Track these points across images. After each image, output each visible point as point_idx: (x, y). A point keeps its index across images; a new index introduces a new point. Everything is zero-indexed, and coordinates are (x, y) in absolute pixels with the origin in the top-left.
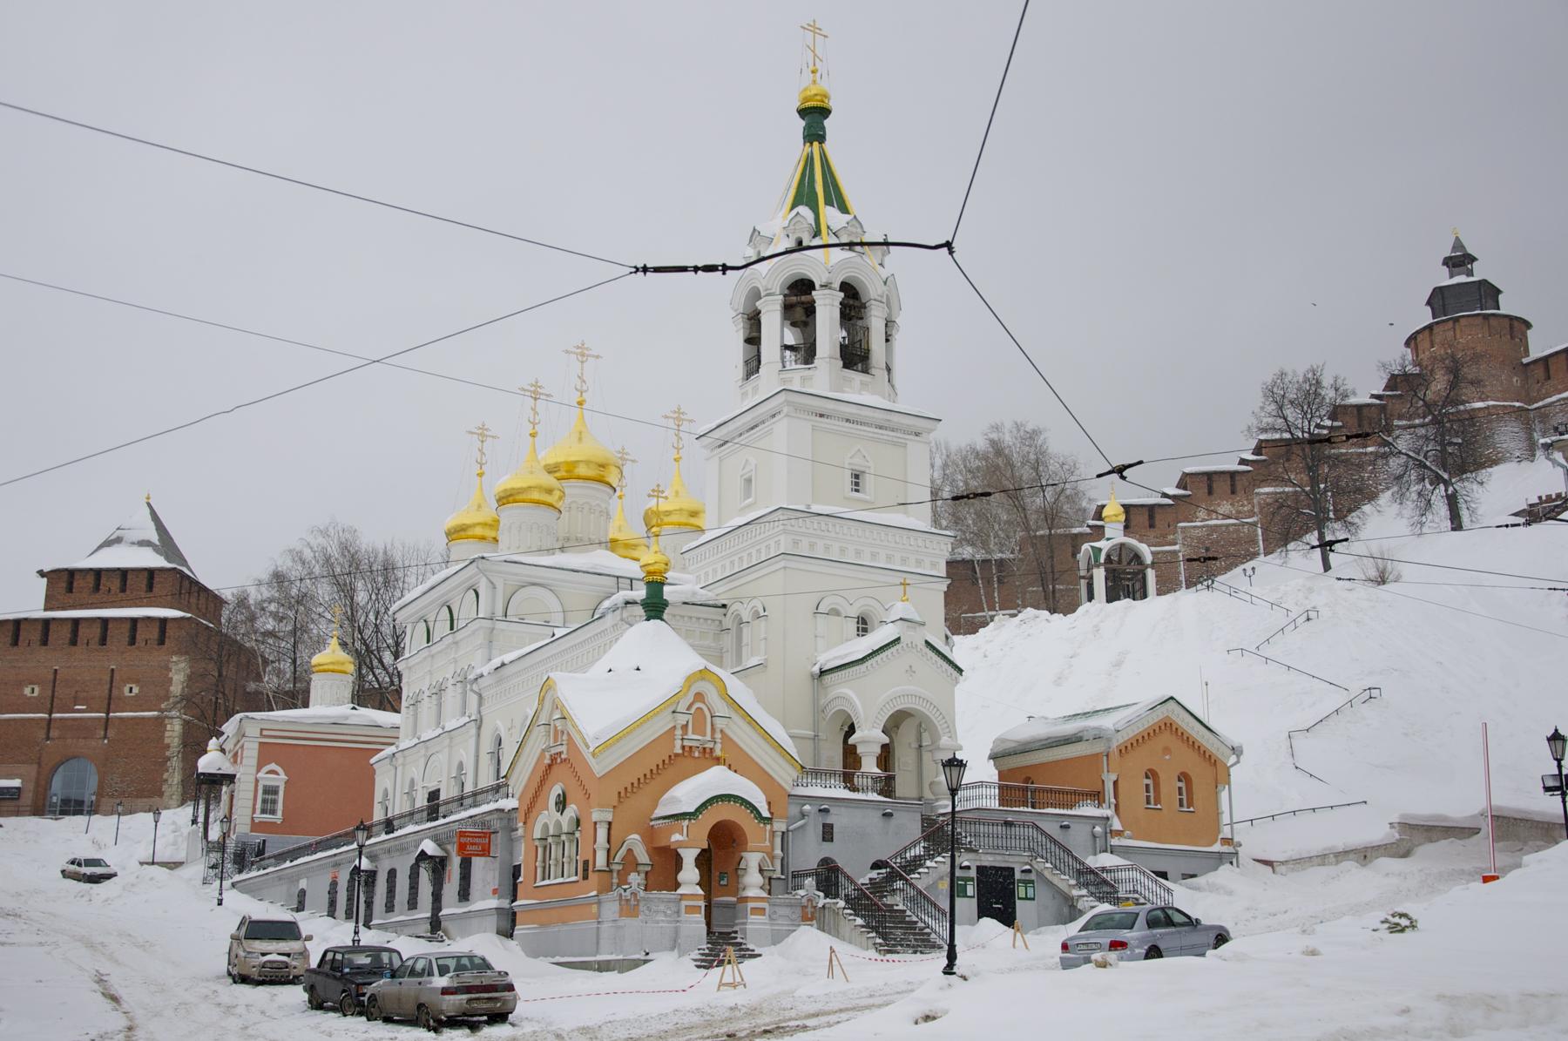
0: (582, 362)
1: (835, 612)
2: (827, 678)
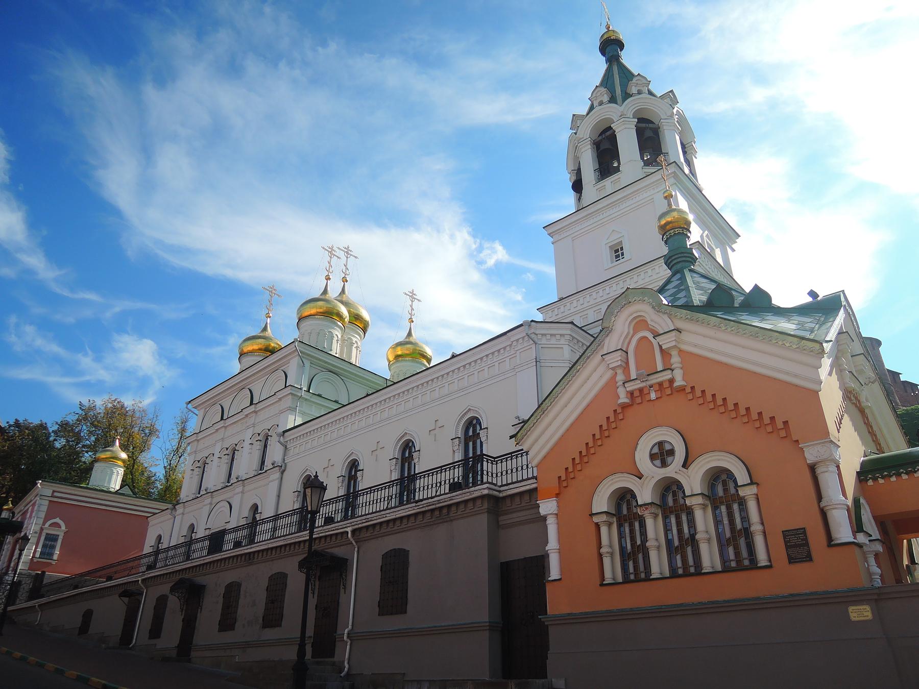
0: (347, 257)
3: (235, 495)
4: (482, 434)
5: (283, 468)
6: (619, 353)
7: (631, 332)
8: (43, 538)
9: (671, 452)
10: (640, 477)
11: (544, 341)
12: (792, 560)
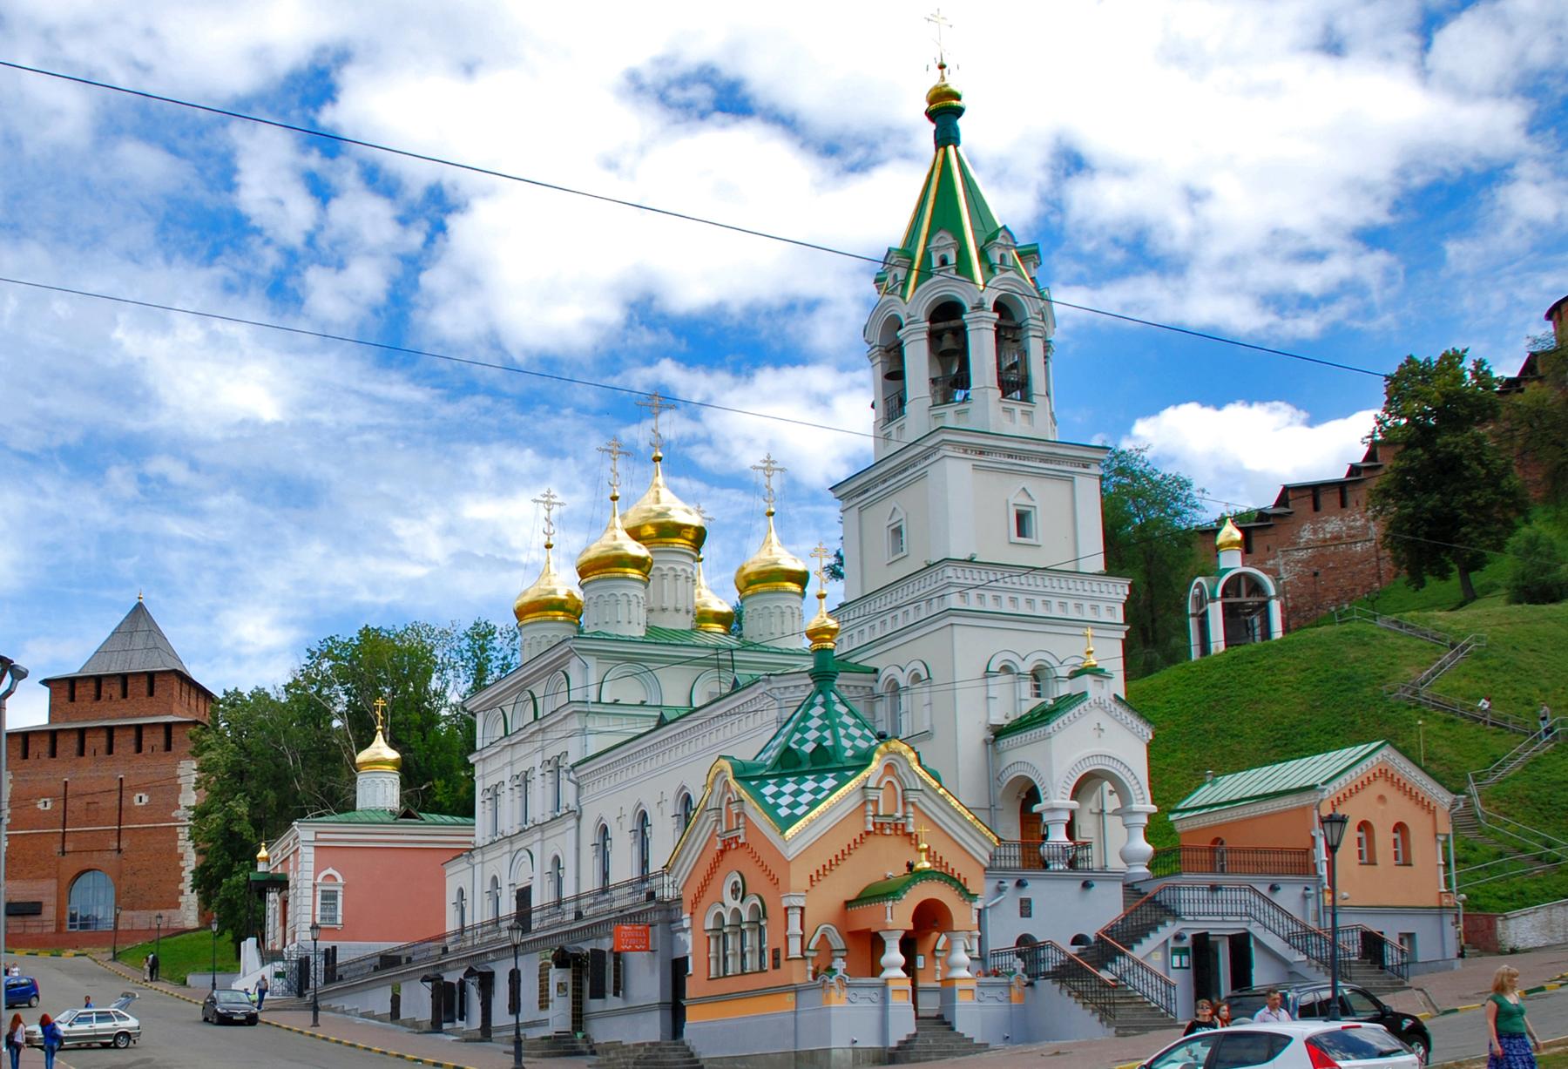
1: (1006, 669)
2: (1004, 743)
3: (533, 841)
5: (578, 813)
8: (319, 898)
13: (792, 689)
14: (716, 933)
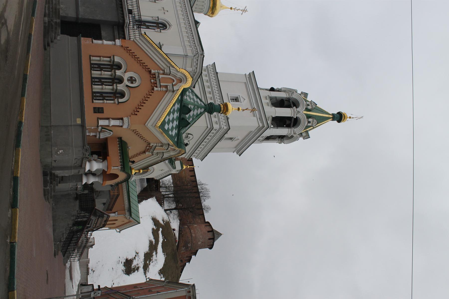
4: (159, 30)
6: (169, 72)
7: (177, 78)
9: (132, 83)
10: (125, 72)
11: (195, 60)
12: (94, 108)
13: (197, 62)
14: (112, 61)
